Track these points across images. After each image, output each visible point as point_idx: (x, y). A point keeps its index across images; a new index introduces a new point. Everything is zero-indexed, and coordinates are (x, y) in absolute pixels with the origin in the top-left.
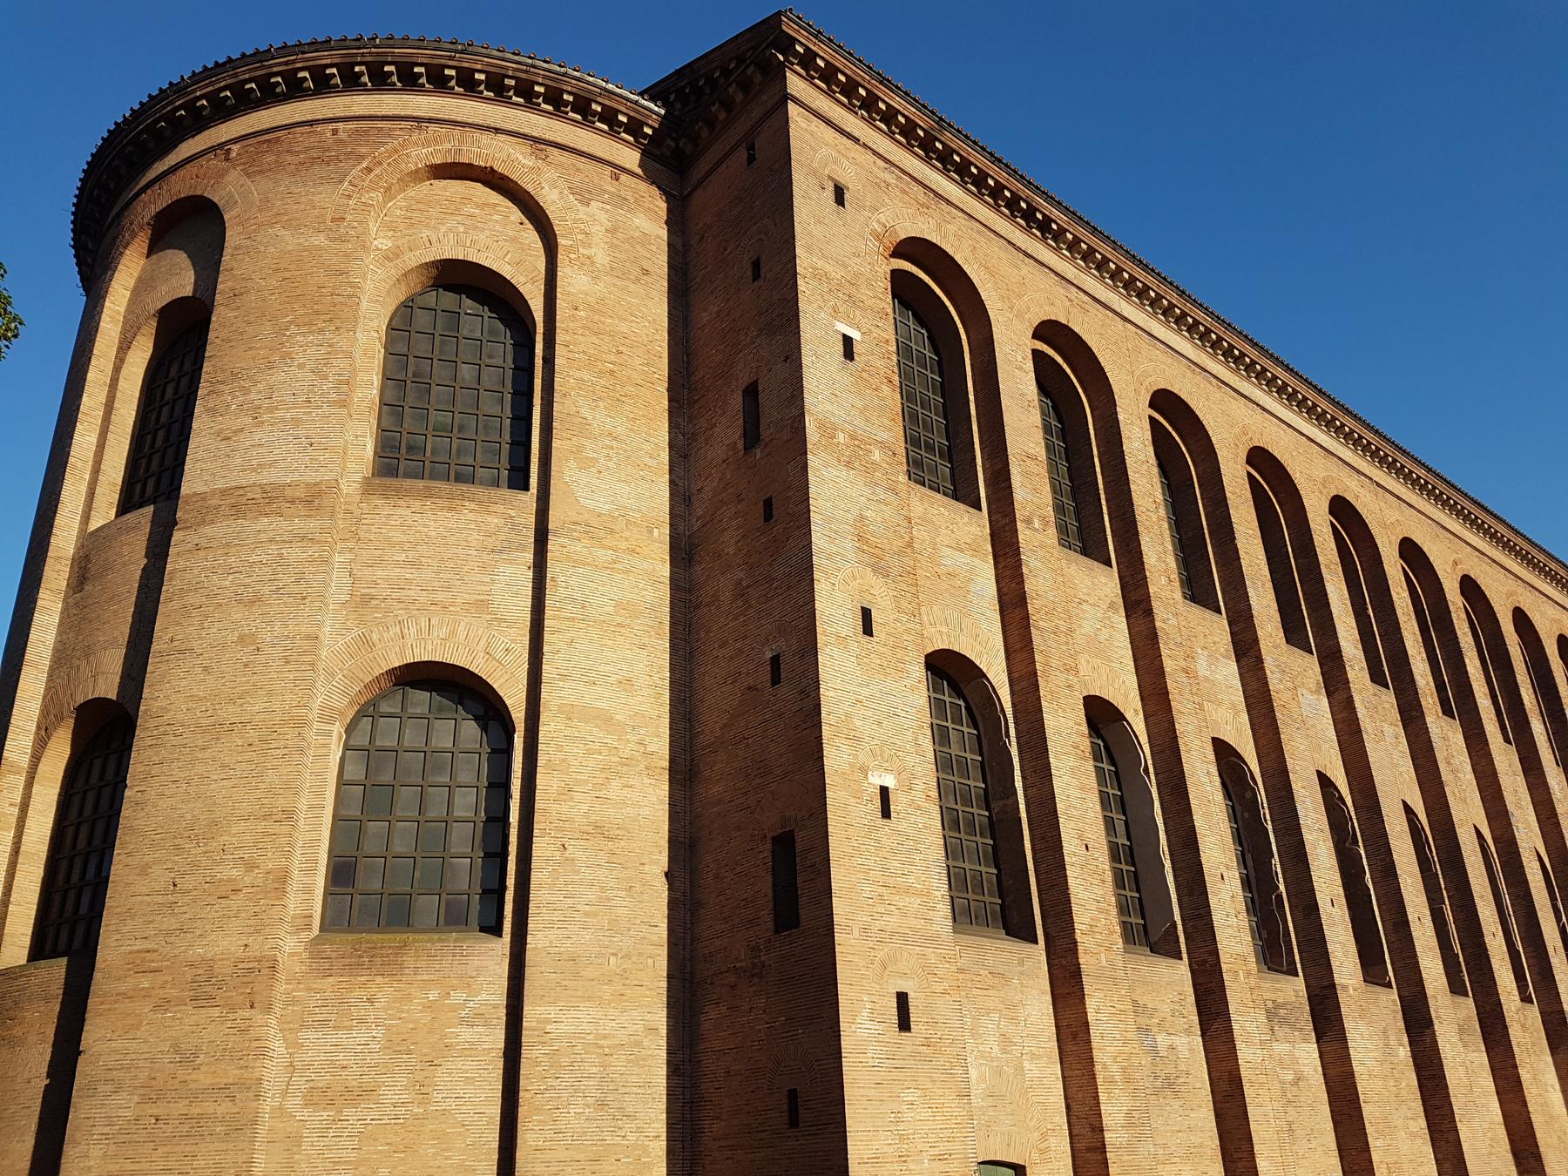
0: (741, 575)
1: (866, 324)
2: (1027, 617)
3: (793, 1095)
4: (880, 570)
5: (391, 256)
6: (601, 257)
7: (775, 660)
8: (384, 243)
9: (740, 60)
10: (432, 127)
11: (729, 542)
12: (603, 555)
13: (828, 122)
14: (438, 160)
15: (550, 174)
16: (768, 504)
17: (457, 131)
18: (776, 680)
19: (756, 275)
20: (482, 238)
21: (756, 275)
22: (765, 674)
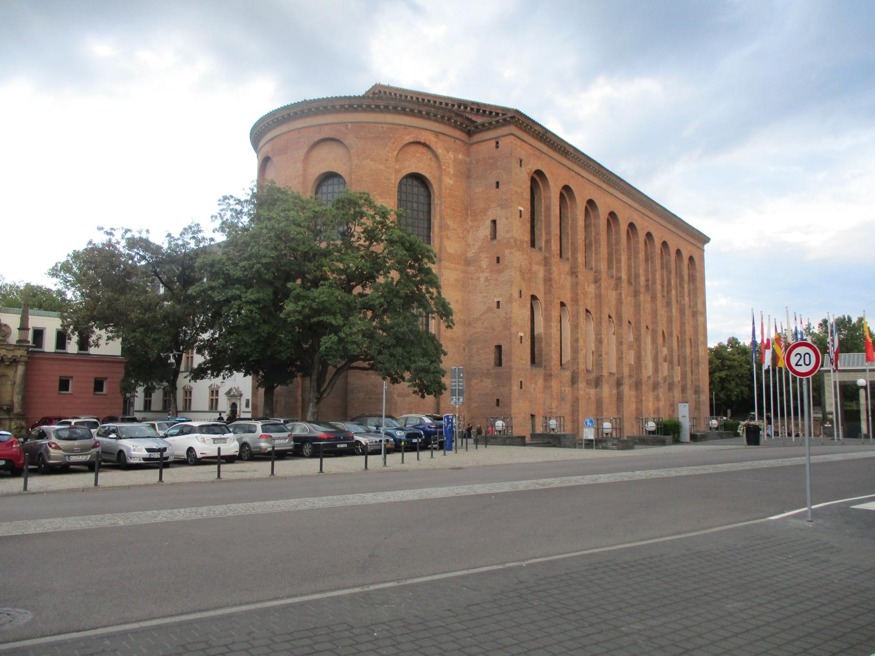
0: (487, 275)
2: (551, 285)
3: (498, 400)
4: (524, 279)
5: (398, 171)
6: (452, 172)
7: (498, 302)
8: (397, 167)
9: (497, 114)
10: (410, 129)
11: (484, 264)
12: (452, 265)
14: (411, 140)
16: (498, 258)
18: (498, 307)
19: (497, 187)
21: (497, 187)
22: (495, 305)
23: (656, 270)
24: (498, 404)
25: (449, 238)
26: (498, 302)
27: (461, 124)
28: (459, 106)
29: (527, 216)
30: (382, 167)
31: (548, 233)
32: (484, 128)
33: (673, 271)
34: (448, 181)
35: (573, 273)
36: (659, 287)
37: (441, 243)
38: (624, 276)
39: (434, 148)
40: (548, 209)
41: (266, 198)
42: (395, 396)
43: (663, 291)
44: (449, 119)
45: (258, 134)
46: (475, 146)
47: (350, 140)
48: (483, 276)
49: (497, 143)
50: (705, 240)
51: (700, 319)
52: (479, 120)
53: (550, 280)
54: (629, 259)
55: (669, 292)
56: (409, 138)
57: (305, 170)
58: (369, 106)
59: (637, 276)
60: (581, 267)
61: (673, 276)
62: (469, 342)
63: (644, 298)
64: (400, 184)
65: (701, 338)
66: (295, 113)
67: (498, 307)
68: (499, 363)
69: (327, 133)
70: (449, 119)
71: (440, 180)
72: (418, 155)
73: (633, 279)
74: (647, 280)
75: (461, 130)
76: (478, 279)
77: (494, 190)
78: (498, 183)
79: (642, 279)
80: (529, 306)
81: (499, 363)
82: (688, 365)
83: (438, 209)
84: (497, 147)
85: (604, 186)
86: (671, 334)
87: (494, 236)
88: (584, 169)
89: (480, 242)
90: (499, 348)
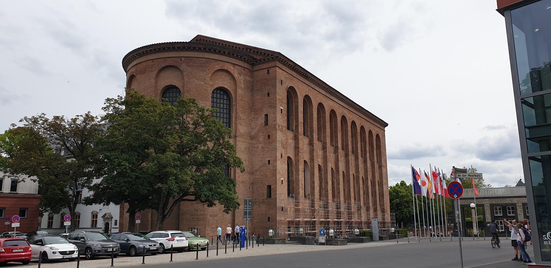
1: (284, 106)
4: (283, 148)
5: (212, 86)
6: (243, 86)
7: (269, 161)
8: (211, 83)
9: (268, 55)
11: (261, 139)
13: (281, 69)
15: (236, 71)
16: (269, 136)
17: (222, 63)
18: (269, 163)
19: (268, 96)
20: (225, 82)
21: (268, 96)
23: (357, 142)
24: (269, 220)
25: (241, 124)
26: (269, 161)
27: (248, 60)
28: (247, 50)
29: (285, 112)
30: (202, 83)
31: (297, 121)
32: (260, 62)
33: (367, 143)
34: (240, 91)
35: (311, 144)
36: (359, 151)
37: (236, 127)
38: (340, 146)
39: (232, 72)
40: (297, 108)
41: (132, 100)
42: (208, 216)
43: (362, 154)
44: (241, 57)
45: (127, 61)
46: (256, 72)
47: (183, 67)
48: (260, 146)
49: (268, 71)
50: (386, 125)
51: (383, 169)
52: (258, 58)
53: (298, 148)
54: (342, 136)
55: (366, 154)
56: (218, 67)
57: (156, 83)
58: (195, 48)
59: (347, 145)
60: (315, 141)
61: (368, 145)
62: (252, 184)
63: (352, 158)
64: (213, 92)
65: (384, 181)
66: (150, 50)
67: (269, 163)
68: (269, 195)
69: (169, 62)
70: (241, 57)
71: (236, 92)
72: (223, 77)
73: (345, 147)
74: (353, 148)
75: (247, 63)
76: (258, 147)
77: (266, 98)
78: (268, 94)
79: (350, 147)
80: (286, 162)
81: (269, 195)
82: (378, 196)
83: (234, 108)
84: (268, 73)
85: (328, 95)
86: (367, 179)
87: (266, 123)
88: (317, 85)
89: (259, 127)
90: (269, 187)
